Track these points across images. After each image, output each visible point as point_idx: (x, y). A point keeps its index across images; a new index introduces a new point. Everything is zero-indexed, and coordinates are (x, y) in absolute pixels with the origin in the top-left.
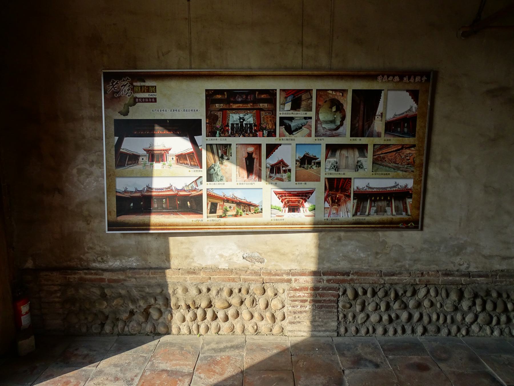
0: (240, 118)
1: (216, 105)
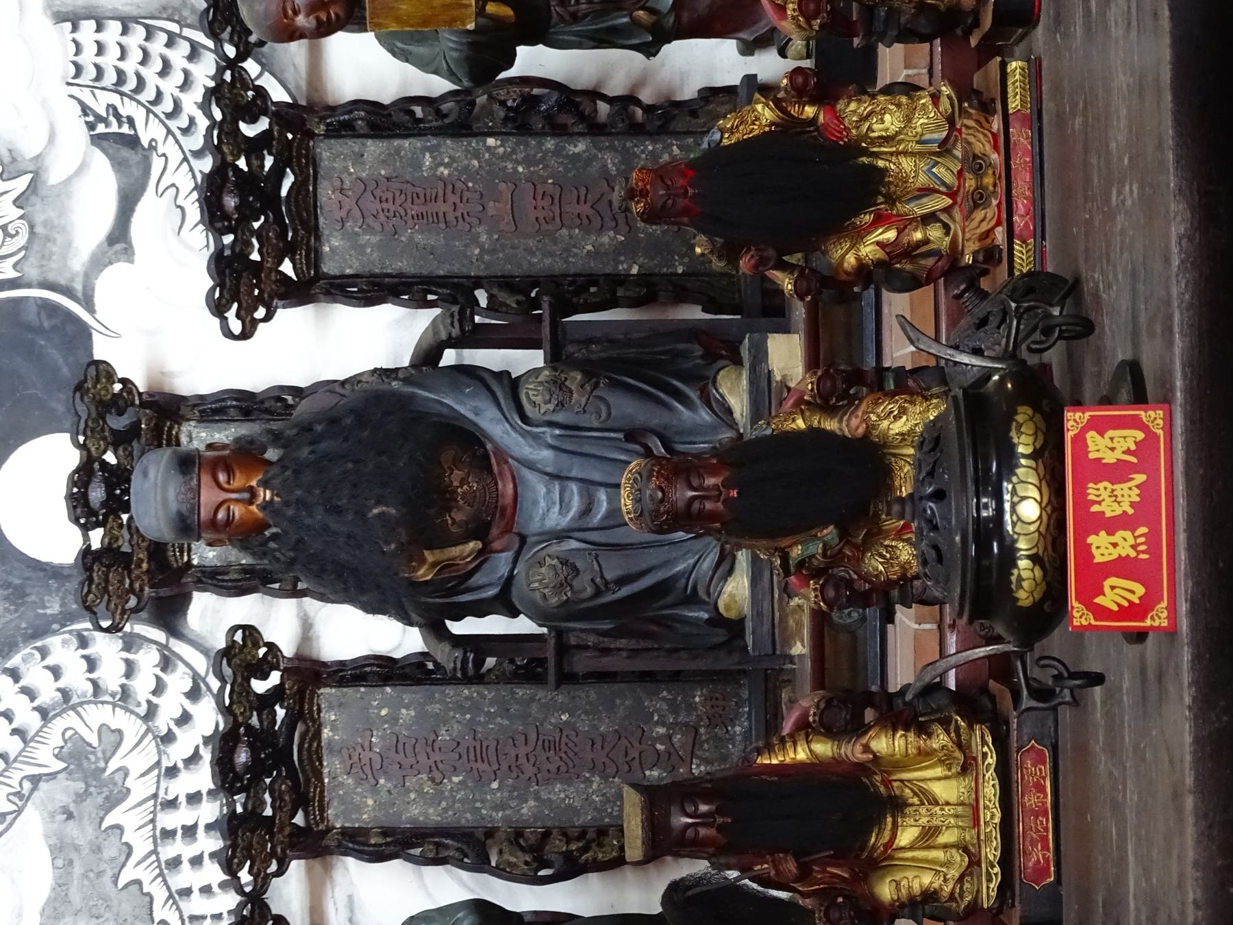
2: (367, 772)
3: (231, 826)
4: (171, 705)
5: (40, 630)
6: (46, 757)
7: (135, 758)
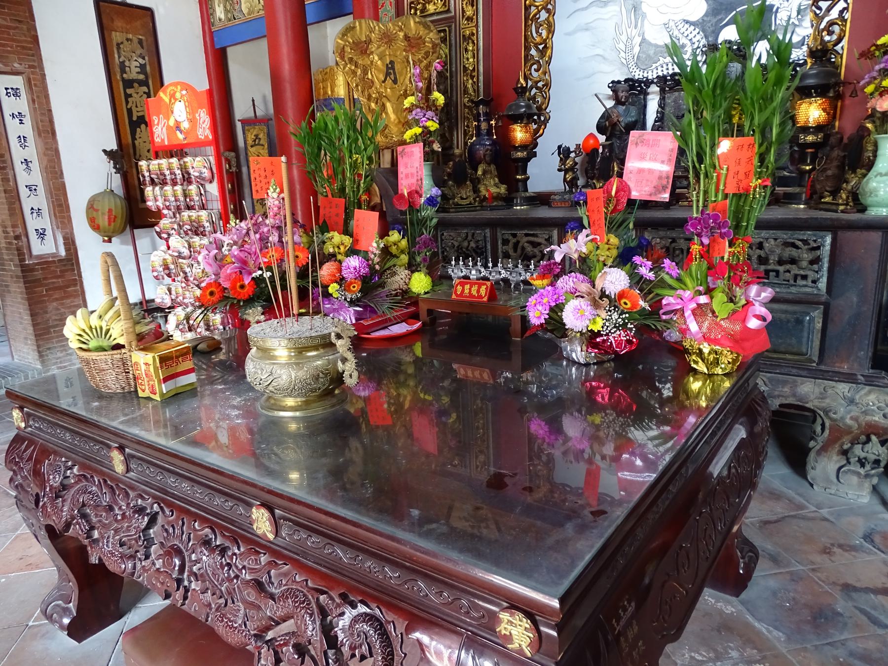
2: (675, 101)
3: (664, 77)
5: (706, 37)
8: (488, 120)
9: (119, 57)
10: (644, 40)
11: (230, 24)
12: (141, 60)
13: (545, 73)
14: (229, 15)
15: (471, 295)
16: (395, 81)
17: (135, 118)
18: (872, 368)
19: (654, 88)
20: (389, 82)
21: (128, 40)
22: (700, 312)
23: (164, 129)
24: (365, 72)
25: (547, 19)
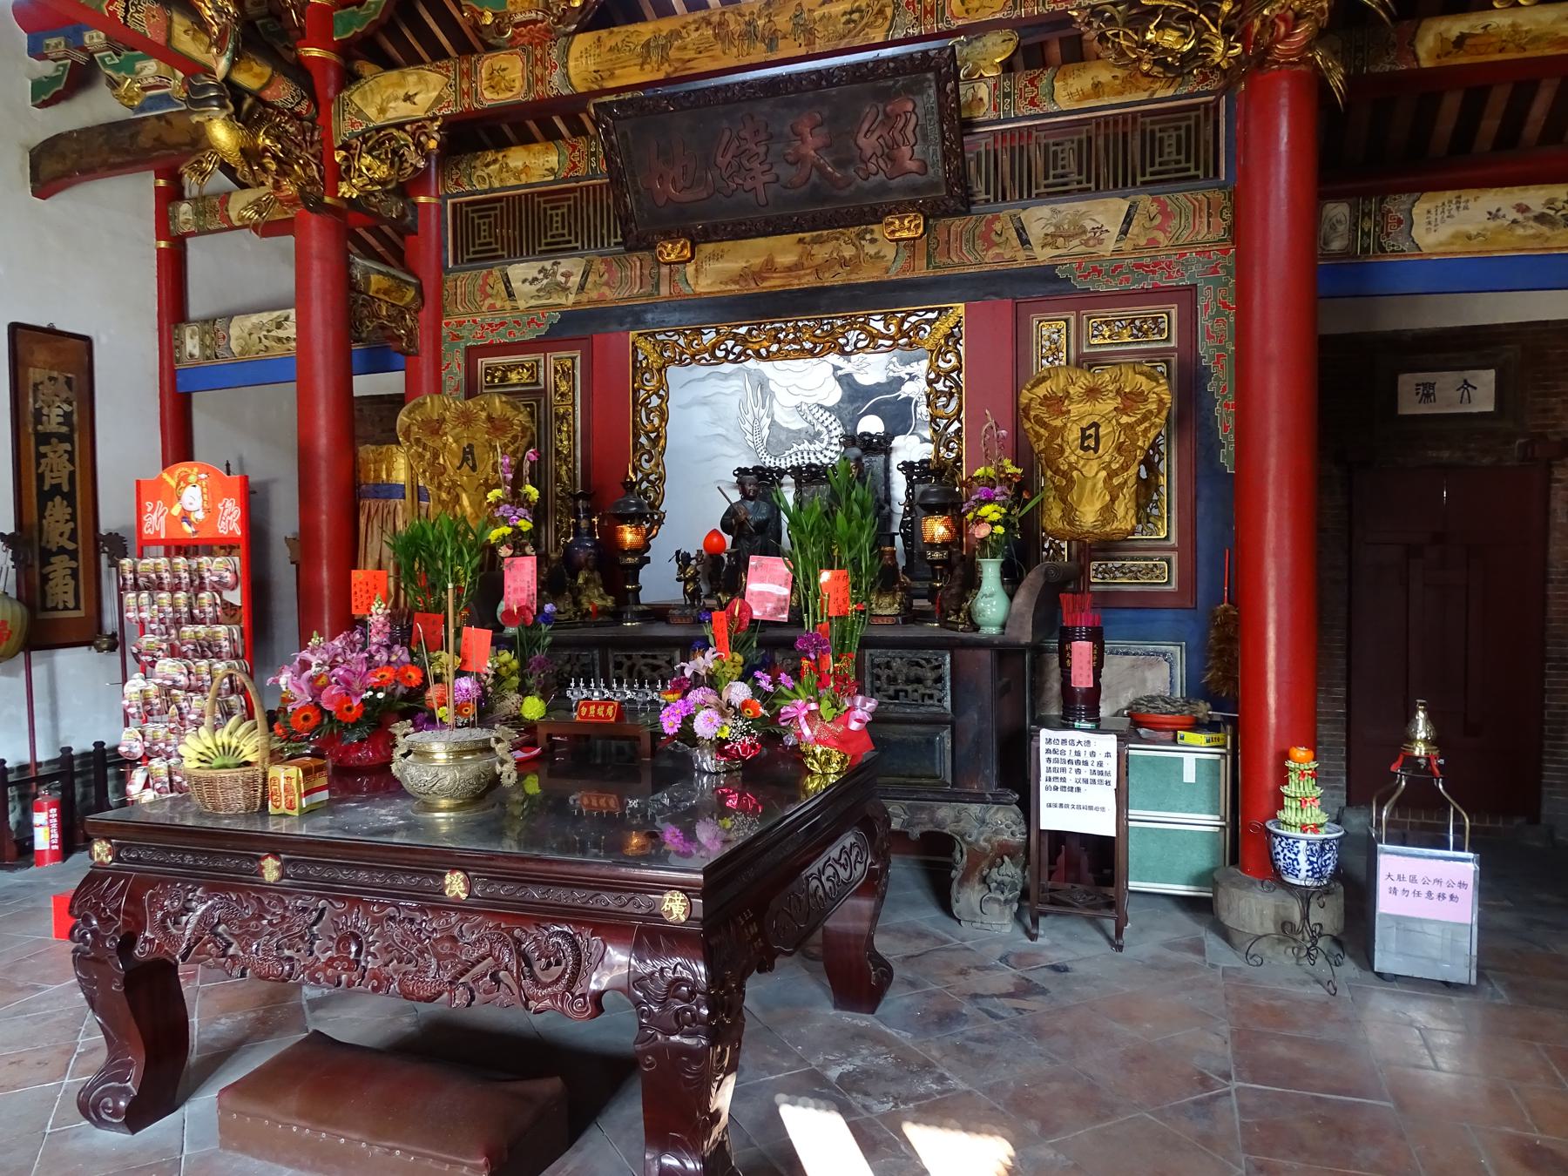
0: (856, 395)
1: (520, 272)
3: (799, 467)
4: (828, 453)
6: (818, 427)
7: (818, 446)
8: (589, 518)
9: (35, 402)
10: (773, 424)
11: (208, 363)
12: (66, 407)
13: (657, 465)
14: (208, 352)
15: (597, 716)
16: (474, 468)
17: (46, 488)
18: (999, 786)
19: (788, 479)
20: (466, 468)
21: (51, 379)
22: (812, 717)
23: (162, 519)
24: (436, 456)
25: (660, 406)
